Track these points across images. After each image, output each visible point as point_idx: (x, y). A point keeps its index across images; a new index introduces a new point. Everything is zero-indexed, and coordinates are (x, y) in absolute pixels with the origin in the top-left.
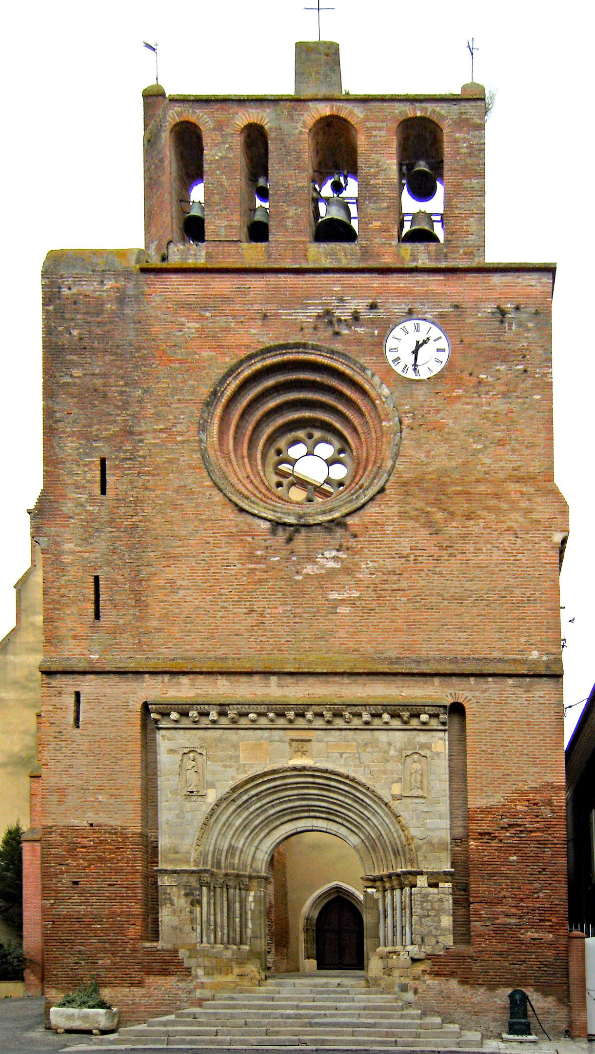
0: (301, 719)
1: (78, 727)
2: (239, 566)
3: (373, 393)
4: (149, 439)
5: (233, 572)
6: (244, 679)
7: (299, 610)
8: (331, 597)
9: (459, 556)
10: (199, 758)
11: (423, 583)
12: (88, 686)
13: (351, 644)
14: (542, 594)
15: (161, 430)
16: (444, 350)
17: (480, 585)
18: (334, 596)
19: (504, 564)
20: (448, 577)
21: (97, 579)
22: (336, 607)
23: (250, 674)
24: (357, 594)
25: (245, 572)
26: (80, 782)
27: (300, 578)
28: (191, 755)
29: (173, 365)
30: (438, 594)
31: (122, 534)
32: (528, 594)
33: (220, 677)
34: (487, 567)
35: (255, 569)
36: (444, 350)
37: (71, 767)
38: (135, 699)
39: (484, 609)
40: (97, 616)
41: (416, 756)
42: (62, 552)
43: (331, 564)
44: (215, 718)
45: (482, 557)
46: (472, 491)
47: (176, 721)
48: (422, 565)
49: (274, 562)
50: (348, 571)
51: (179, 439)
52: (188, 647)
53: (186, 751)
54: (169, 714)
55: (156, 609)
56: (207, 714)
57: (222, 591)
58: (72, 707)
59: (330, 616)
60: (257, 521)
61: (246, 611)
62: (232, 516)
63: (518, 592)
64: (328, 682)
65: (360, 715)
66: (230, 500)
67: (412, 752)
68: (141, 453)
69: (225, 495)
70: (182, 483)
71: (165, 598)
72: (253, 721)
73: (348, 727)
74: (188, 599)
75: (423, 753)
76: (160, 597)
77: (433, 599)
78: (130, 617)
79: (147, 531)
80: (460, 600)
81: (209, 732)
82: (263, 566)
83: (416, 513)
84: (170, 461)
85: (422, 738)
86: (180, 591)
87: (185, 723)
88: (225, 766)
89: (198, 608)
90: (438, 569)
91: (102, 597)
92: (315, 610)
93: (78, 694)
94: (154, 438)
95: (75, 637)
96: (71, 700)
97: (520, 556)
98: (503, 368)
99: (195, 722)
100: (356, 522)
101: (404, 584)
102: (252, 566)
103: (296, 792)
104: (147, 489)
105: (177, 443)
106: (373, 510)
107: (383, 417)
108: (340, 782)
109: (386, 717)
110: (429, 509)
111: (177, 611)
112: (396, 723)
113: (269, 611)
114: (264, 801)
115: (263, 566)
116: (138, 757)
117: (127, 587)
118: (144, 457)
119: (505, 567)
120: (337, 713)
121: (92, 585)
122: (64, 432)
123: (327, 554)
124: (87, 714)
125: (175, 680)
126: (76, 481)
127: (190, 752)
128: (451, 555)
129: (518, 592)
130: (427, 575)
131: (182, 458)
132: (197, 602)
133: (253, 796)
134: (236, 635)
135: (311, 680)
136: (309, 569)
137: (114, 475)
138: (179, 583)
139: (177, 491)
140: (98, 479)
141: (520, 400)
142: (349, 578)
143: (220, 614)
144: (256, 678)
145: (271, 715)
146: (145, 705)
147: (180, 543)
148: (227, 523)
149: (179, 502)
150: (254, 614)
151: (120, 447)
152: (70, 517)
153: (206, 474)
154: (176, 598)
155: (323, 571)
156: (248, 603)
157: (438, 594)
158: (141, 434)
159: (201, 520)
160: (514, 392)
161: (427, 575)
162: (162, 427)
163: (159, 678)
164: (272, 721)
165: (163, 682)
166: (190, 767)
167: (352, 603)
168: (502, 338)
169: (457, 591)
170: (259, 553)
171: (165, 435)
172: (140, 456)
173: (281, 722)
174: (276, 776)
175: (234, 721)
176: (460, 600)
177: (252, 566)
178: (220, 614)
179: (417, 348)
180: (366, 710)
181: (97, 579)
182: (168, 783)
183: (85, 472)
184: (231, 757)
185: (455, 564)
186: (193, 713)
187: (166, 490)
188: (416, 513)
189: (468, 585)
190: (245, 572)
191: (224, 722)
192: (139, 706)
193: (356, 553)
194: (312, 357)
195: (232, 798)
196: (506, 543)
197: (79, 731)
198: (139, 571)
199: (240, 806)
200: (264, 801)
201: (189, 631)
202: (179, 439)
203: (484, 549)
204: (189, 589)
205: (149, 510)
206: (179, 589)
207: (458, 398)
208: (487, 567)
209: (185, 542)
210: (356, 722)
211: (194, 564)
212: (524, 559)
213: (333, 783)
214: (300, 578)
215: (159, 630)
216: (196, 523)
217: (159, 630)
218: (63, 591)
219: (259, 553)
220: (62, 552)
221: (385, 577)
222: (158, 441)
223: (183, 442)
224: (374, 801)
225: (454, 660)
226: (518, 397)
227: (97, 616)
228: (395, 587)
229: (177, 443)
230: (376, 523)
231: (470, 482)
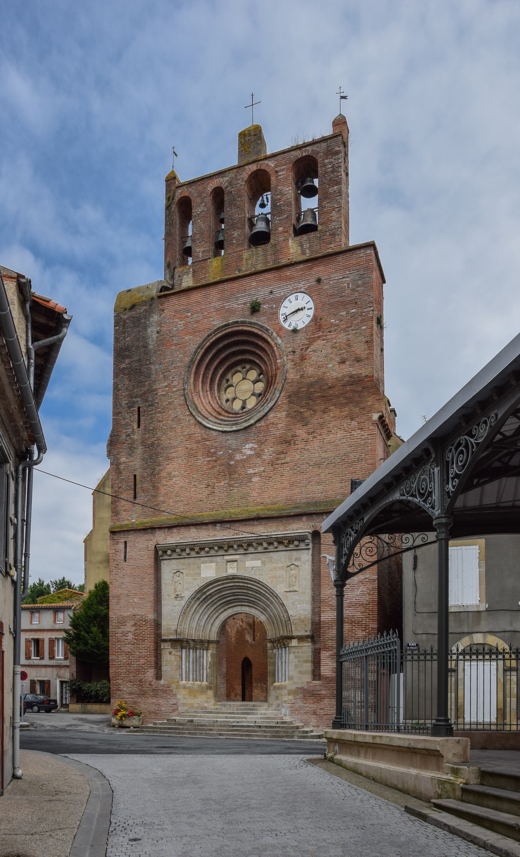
0: (231, 549)
1: (126, 561)
2: (202, 460)
3: (272, 343)
4: (160, 392)
5: (199, 464)
6: (204, 527)
7: (232, 482)
8: (249, 472)
9: (319, 437)
10: (181, 575)
11: (298, 457)
12: (131, 538)
13: (259, 500)
14: (366, 455)
15: (166, 386)
16: (311, 308)
17: (329, 454)
18: (251, 471)
19: (344, 438)
20: (313, 451)
21: (135, 476)
22: (251, 479)
23: (206, 524)
24: (262, 469)
25: (205, 463)
26: (126, 592)
27: (233, 463)
28: (178, 573)
29: (172, 348)
30: (307, 463)
31: (147, 449)
32: (358, 456)
33: (192, 527)
34: (334, 442)
35: (211, 461)
36: (311, 308)
37: (122, 583)
38: (152, 543)
39: (332, 469)
40: (135, 497)
41: (293, 566)
42: (120, 464)
43: (249, 452)
44: (189, 552)
45: (331, 436)
46: (326, 395)
47: (170, 555)
48: (298, 446)
49: (220, 455)
50: (258, 455)
51: (174, 389)
52: (177, 511)
53: (175, 571)
54: (166, 552)
55: (162, 491)
56: (185, 550)
57: (194, 476)
58: (123, 550)
59: (248, 484)
60: (212, 432)
61: (205, 486)
62: (199, 431)
63: (351, 455)
64: (246, 525)
65: (262, 544)
66: (198, 422)
67: (290, 563)
68: (156, 401)
69: (196, 419)
70: (175, 416)
71: (166, 483)
72: (208, 552)
73: (256, 551)
74: (177, 482)
75: (296, 564)
76: (164, 483)
77: (304, 466)
78: (150, 496)
79: (159, 445)
80: (318, 465)
81: (186, 560)
82: (214, 458)
83: (295, 414)
84: (170, 403)
85: (295, 554)
86: (174, 479)
87: (175, 556)
88: (194, 579)
89: (182, 487)
90: (307, 447)
91: (138, 486)
92: (240, 481)
93: (126, 542)
94: (163, 392)
95: (125, 511)
96: (122, 546)
97: (353, 432)
98: (343, 313)
99: (180, 555)
100: (263, 425)
101: (288, 459)
102: (208, 459)
103: (230, 591)
104: (160, 421)
105: (173, 392)
106: (272, 415)
107: (278, 357)
108: (253, 585)
109: (276, 544)
110: (302, 410)
111: (172, 490)
112: (281, 547)
113: (216, 484)
114: (214, 598)
115: (214, 458)
116: (153, 576)
117: (149, 479)
118: (157, 403)
119: (344, 440)
120: (246, 546)
121: (132, 480)
122: (121, 396)
123: (247, 446)
124: (130, 554)
125: (170, 531)
126: (127, 422)
127: (177, 572)
128: (314, 437)
129: (351, 455)
130: (301, 452)
131: (176, 401)
132: (181, 484)
133: (208, 596)
134: (200, 501)
135: (237, 525)
136: (238, 457)
137: (144, 416)
138: (174, 473)
139: (173, 420)
140: (137, 419)
141: (354, 331)
142: (259, 459)
143: (193, 489)
144: (210, 526)
145: (216, 548)
146: (156, 547)
147: (174, 450)
148: (197, 435)
149: (174, 426)
150: (210, 488)
151: (147, 399)
152: (124, 443)
153: (186, 408)
154: (171, 483)
155: (245, 457)
156: (206, 481)
157: (307, 463)
158: (156, 390)
159: (184, 435)
160: (350, 327)
161: (301, 452)
162: (166, 384)
163: (163, 531)
164: (217, 551)
165: (164, 532)
166: (176, 581)
167: (259, 474)
168: (344, 294)
169: (318, 460)
170: (212, 450)
171: (167, 389)
172: (156, 403)
173: (221, 552)
174: (219, 583)
175: (198, 553)
176: (318, 465)
177: (208, 459)
178: (193, 489)
179: (297, 310)
180: (265, 541)
181: (135, 476)
182: (167, 590)
183: (131, 417)
184: (197, 574)
185: (316, 443)
186: (178, 550)
187: (168, 420)
188: (295, 414)
189: (323, 455)
190: (205, 463)
191: (193, 554)
192: (153, 547)
193: (263, 443)
194: (241, 328)
195: (197, 597)
196: (345, 425)
197: (126, 563)
198: (155, 469)
199: (202, 602)
200: (214, 598)
201: (177, 501)
202: (174, 389)
203: (333, 431)
204: (178, 477)
205: (159, 433)
206: (173, 477)
207: (319, 337)
208: (334, 442)
209: (176, 449)
210: (260, 549)
211: (180, 462)
212: (356, 434)
213: (249, 586)
214: (233, 463)
215: (164, 502)
216: (182, 438)
217: (164, 502)
218: (120, 485)
219: (212, 450)
220: (120, 464)
221: (278, 456)
222: (164, 393)
223: (176, 391)
224: (270, 595)
225: (316, 504)
226: (353, 330)
227: (135, 497)
228: (283, 461)
229: (173, 392)
230: (273, 424)
231: (325, 390)
